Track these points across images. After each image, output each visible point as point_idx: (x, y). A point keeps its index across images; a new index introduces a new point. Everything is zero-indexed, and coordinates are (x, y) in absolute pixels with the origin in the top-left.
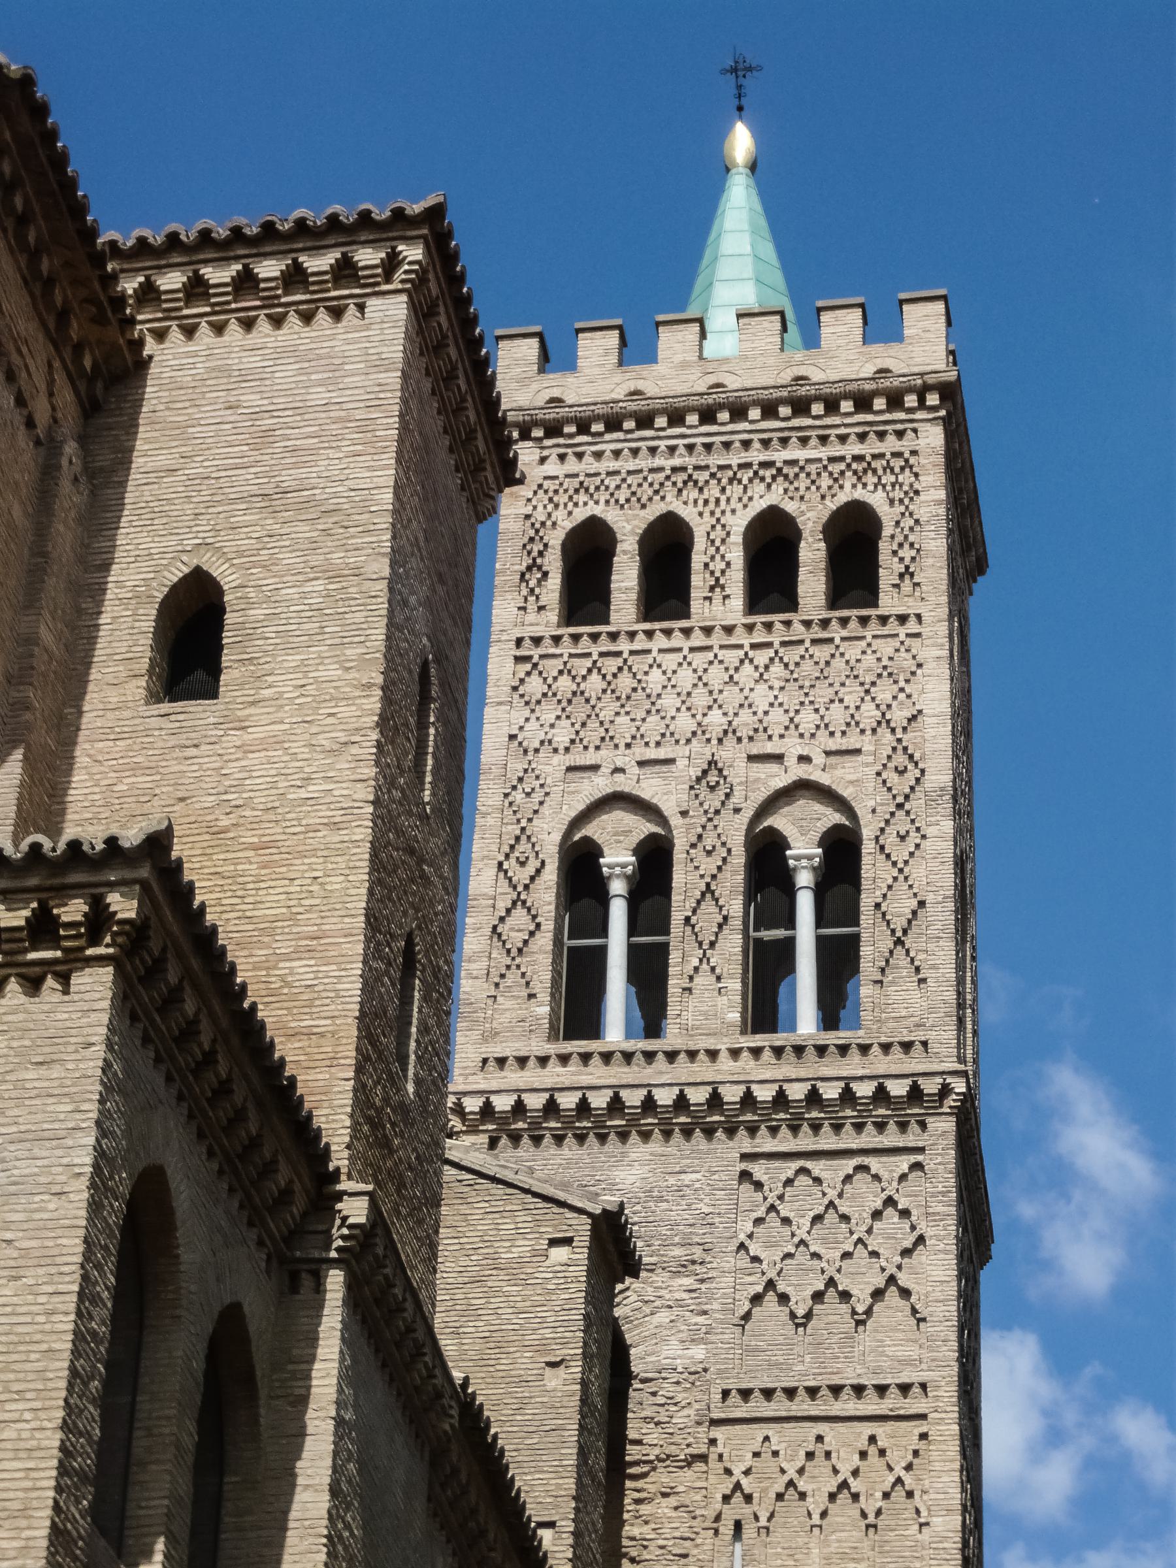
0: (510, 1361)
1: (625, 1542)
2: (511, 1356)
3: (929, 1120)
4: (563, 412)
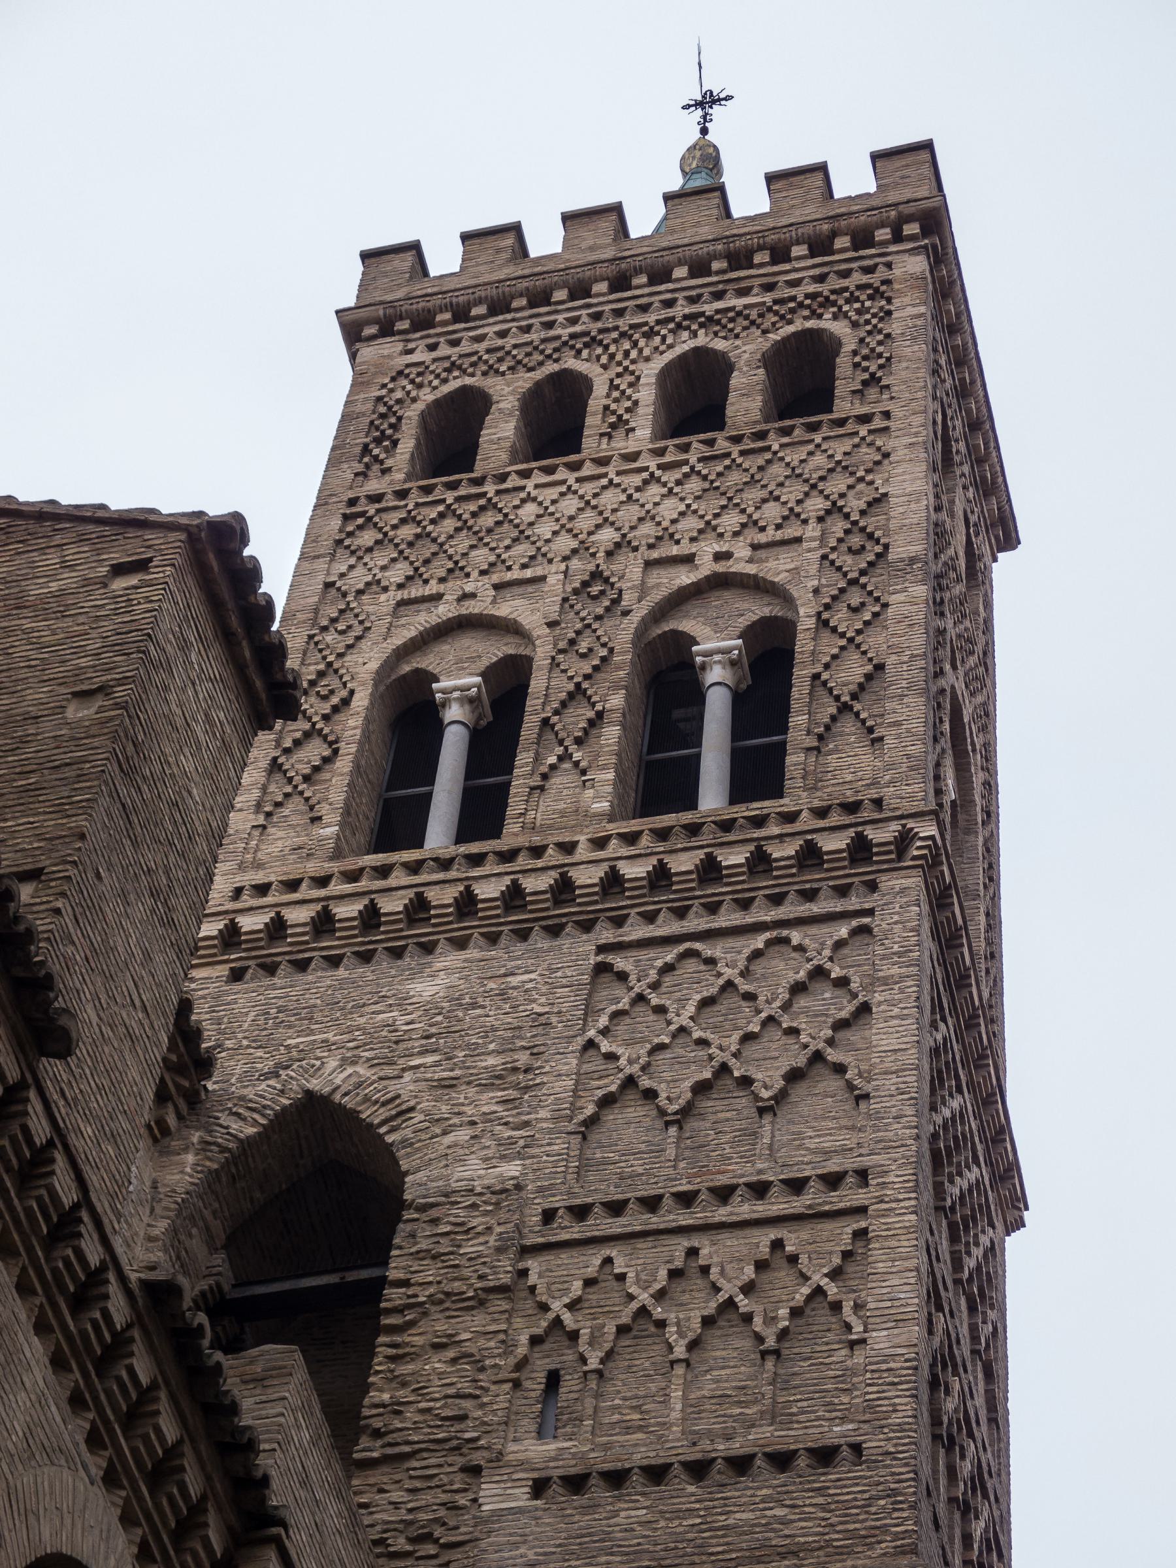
0: (14, 700)
1: (366, 1412)
3: (884, 879)
4: (437, 301)
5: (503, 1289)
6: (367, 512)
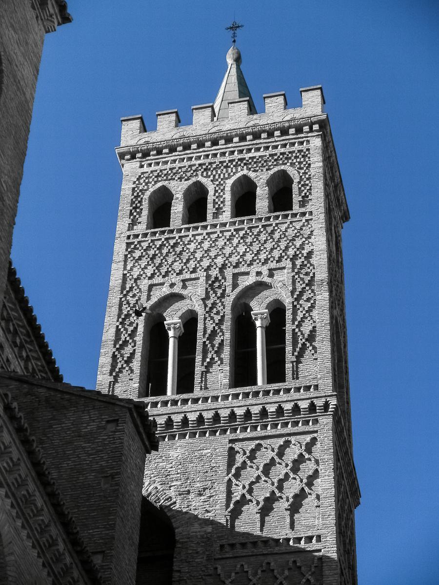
0: (84, 478)
2: (84, 476)
3: (320, 418)
4: (150, 146)
5: (210, 575)
6: (134, 242)
